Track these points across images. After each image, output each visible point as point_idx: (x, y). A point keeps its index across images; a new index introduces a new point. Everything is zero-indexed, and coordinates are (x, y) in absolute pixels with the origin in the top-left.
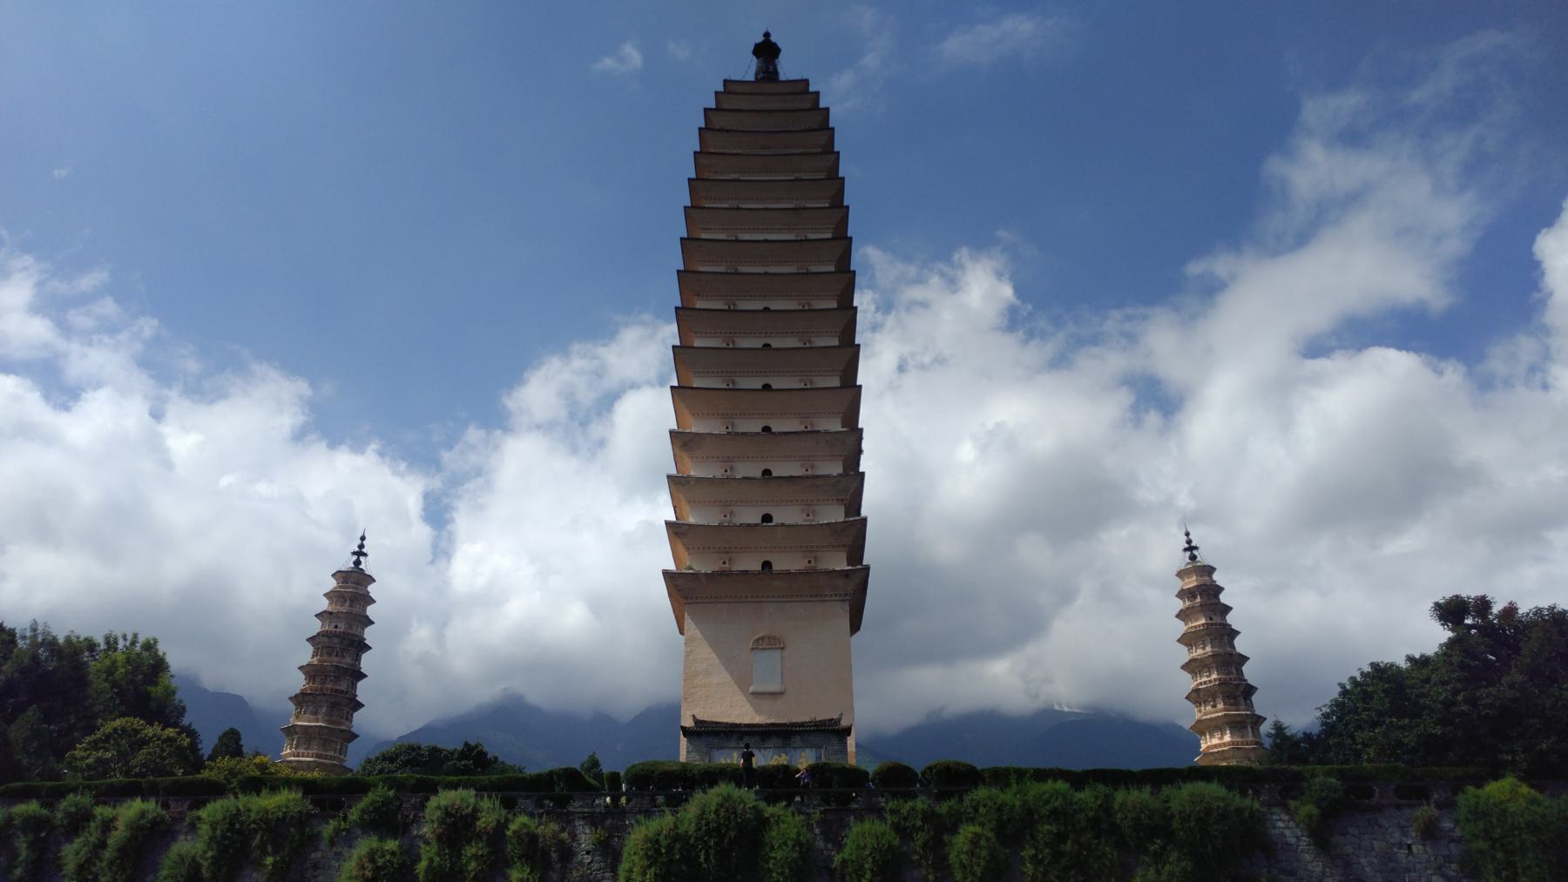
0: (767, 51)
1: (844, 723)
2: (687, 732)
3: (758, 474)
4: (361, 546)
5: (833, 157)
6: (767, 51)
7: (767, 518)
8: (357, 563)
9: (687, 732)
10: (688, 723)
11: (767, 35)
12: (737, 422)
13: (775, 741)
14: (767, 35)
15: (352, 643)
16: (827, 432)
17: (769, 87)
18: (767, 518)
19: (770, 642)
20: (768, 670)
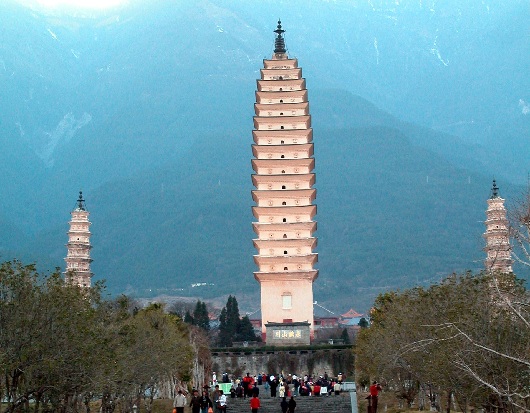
0: (279, 31)
1: (309, 323)
2: (266, 325)
3: (282, 238)
4: (81, 197)
5: (307, 104)
6: (279, 31)
7: (285, 252)
8: (80, 206)
9: (266, 325)
10: (267, 323)
11: (279, 22)
12: (274, 217)
13: (289, 327)
14: (279, 22)
15: (87, 247)
16: (305, 223)
17: (282, 64)
18: (285, 252)
19: (288, 293)
20: (287, 302)
